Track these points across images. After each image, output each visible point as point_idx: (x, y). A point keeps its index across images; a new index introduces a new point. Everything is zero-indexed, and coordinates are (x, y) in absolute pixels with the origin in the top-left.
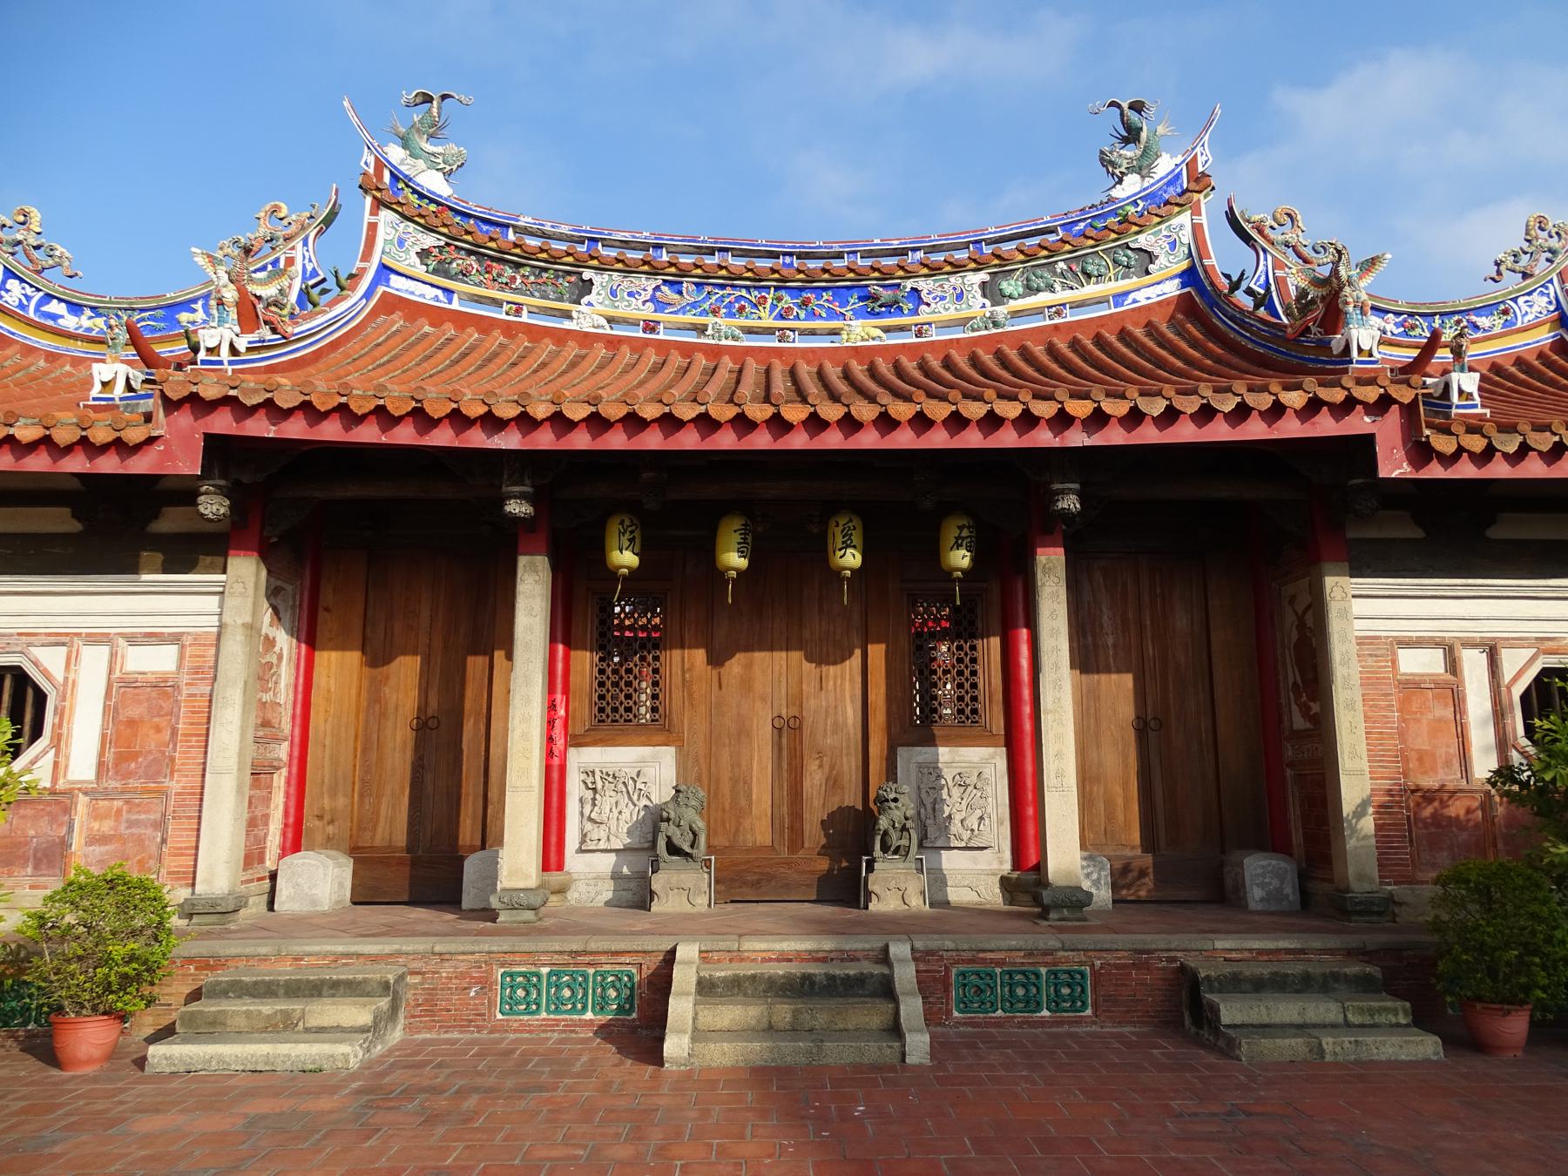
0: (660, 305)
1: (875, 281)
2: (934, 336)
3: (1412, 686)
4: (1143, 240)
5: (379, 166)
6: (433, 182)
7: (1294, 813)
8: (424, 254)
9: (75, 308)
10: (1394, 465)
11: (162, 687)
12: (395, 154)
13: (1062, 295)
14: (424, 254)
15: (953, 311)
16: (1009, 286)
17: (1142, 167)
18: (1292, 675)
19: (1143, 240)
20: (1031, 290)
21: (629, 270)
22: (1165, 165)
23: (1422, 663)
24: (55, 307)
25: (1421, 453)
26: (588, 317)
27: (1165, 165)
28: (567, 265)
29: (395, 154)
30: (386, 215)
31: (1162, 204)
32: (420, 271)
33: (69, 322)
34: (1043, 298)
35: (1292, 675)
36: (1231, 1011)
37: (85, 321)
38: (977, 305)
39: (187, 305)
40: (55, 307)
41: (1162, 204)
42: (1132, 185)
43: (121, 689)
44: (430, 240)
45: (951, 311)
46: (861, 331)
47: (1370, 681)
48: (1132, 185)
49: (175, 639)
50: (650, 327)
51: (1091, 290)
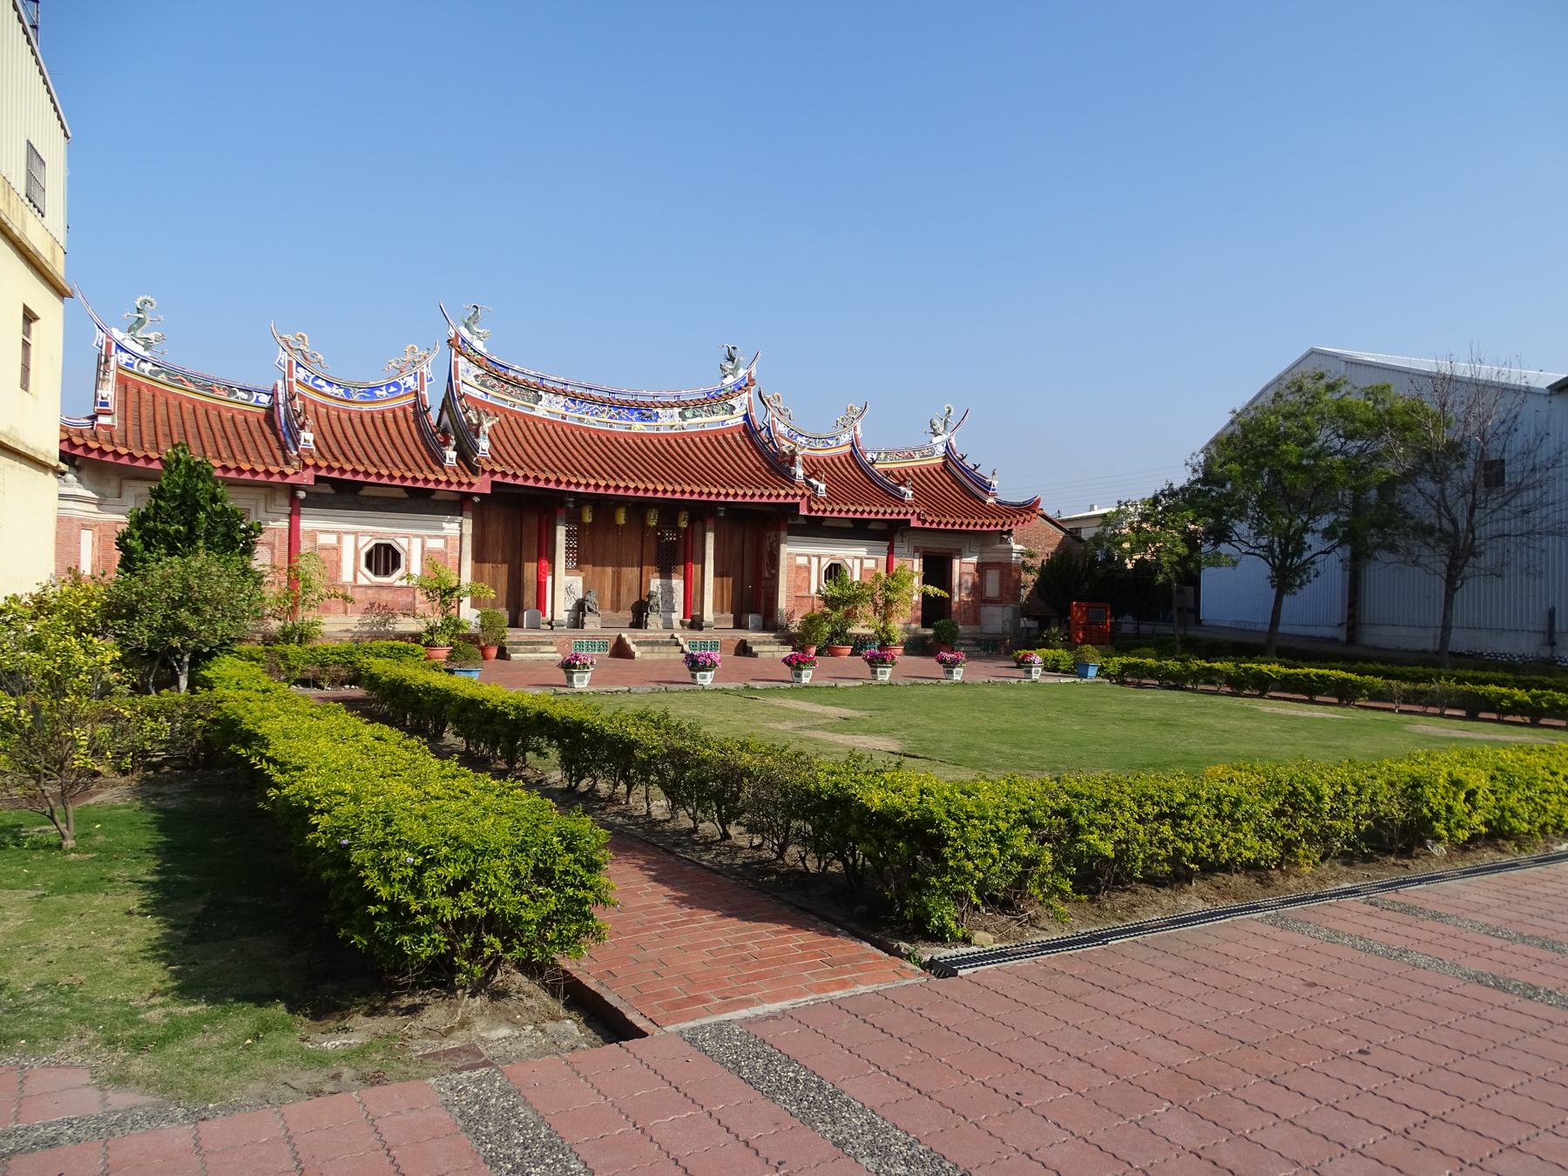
0: (567, 409)
1: (643, 410)
2: (662, 431)
3: (799, 567)
4: (732, 402)
5: (457, 335)
6: (478, 345)
7: (762, 602)
8: (476, 377)
9: (330, 384)
10: (803, 512)
12: (464, 332)
13: (705, 419)
14: (476, 377)
15: (668, 422)
16: (687, 414)
17: (734, 372)
18: (766, 560)
19: (732, 402)
20: (695, 416)
21: (557, 394)
22: (742, 372)
23: (802, 561)
24: (319, 382)
25: (810, 509)
26: (541, 411)
27: (742, 372)
28: (534, 390)
29: (464, 332)
30: (461, 359)
31: (740, 389)
32: (475, 384)
33: (327, 389)
34: (698, 420)
35: (766, 560)
36: (755, 649)
37: (335, 390)
38: (677, 420)
39: (378, 388)
40: (319, 382)
41: (740, 389)
42: (730, 380)
44: (480, 372)
45: (668, 422)
46: (639, 427)
47: (789, 566)
48: (730, 380)
49: (444, 537)
50: (564, 417)
51: (714, 418)
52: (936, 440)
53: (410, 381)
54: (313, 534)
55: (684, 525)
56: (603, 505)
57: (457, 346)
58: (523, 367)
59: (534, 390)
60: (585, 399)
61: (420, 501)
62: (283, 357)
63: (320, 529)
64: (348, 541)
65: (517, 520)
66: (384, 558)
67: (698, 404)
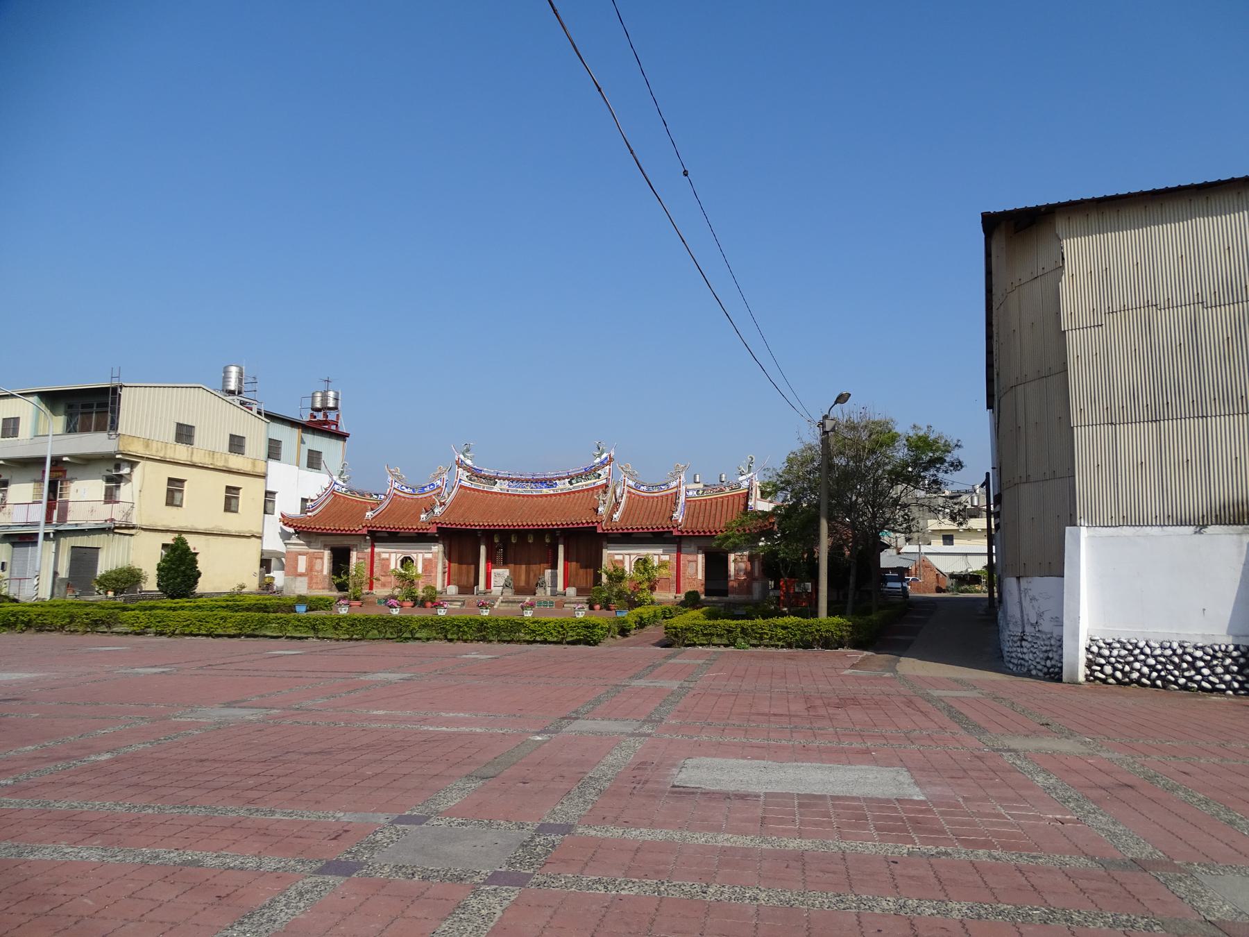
1: (549, 482)
6: (469, 462)
11: (430, 560)
15: (564, 486)
17: (600, 456)
26: (496, 489)
28: (492, 480)
31: (603, 464)
38: (568, 485)
41: (603, 464)
43: (424, 560)
46: (545, 491)
48: (598, 460)
52: (741, 478)
53: (439, 483)
54: (379, 554)
55: (547, 541)
56: (505, 534)
57: (460, 464)
58: (487, 471)
59: (492, 480)
60: (518, 480)
61: (421, 538)
62: (390, 479)
63: (382, 551)
64: (393, 556)
65: (461, 542)
66: (406, 561)
67: (579, 477)
